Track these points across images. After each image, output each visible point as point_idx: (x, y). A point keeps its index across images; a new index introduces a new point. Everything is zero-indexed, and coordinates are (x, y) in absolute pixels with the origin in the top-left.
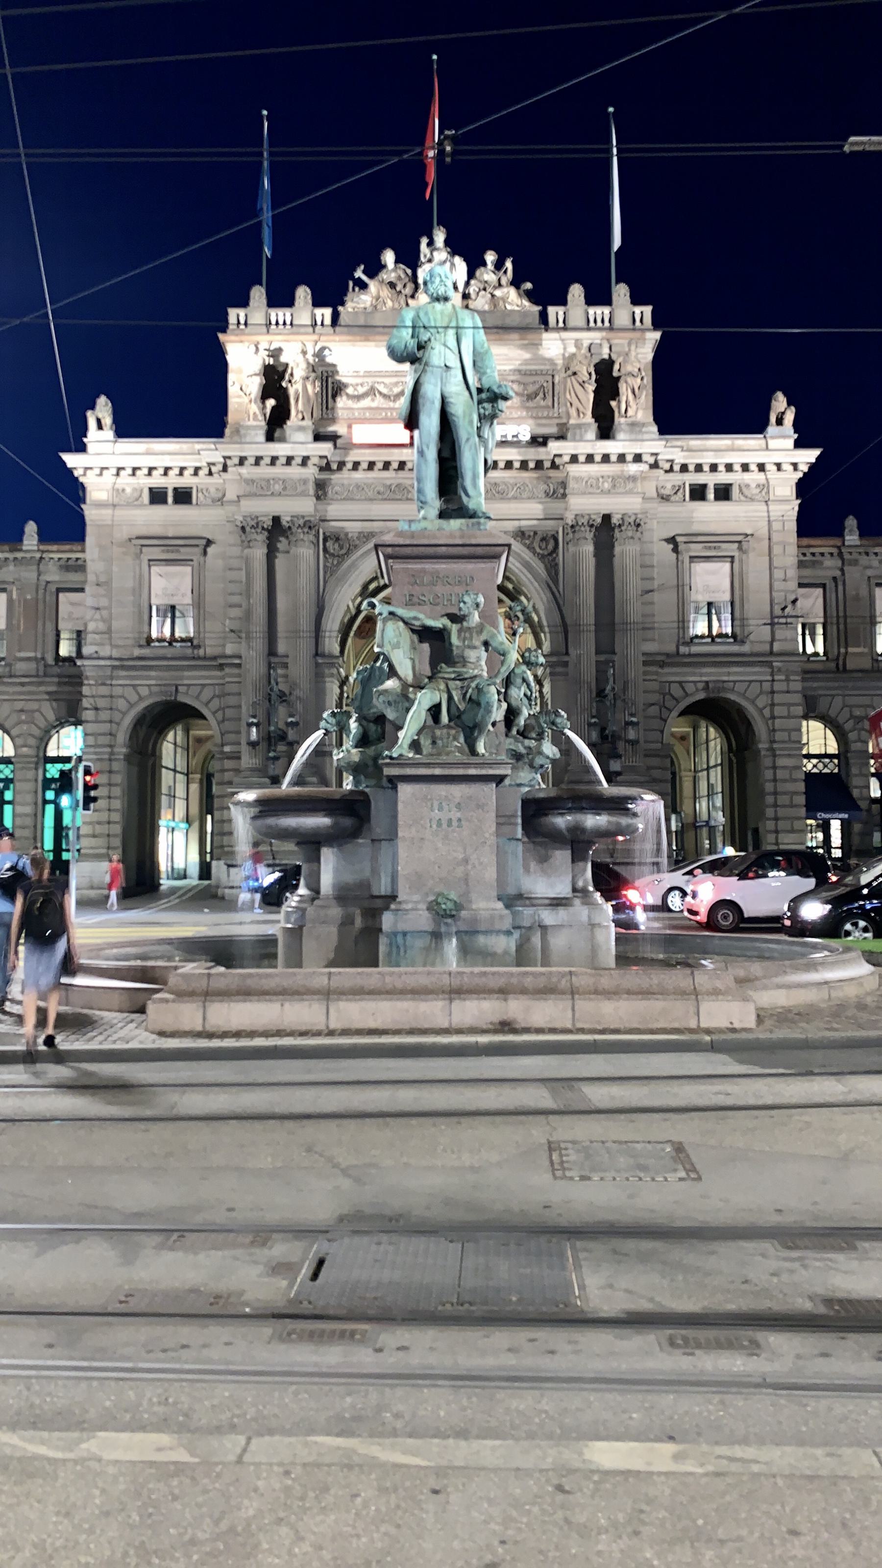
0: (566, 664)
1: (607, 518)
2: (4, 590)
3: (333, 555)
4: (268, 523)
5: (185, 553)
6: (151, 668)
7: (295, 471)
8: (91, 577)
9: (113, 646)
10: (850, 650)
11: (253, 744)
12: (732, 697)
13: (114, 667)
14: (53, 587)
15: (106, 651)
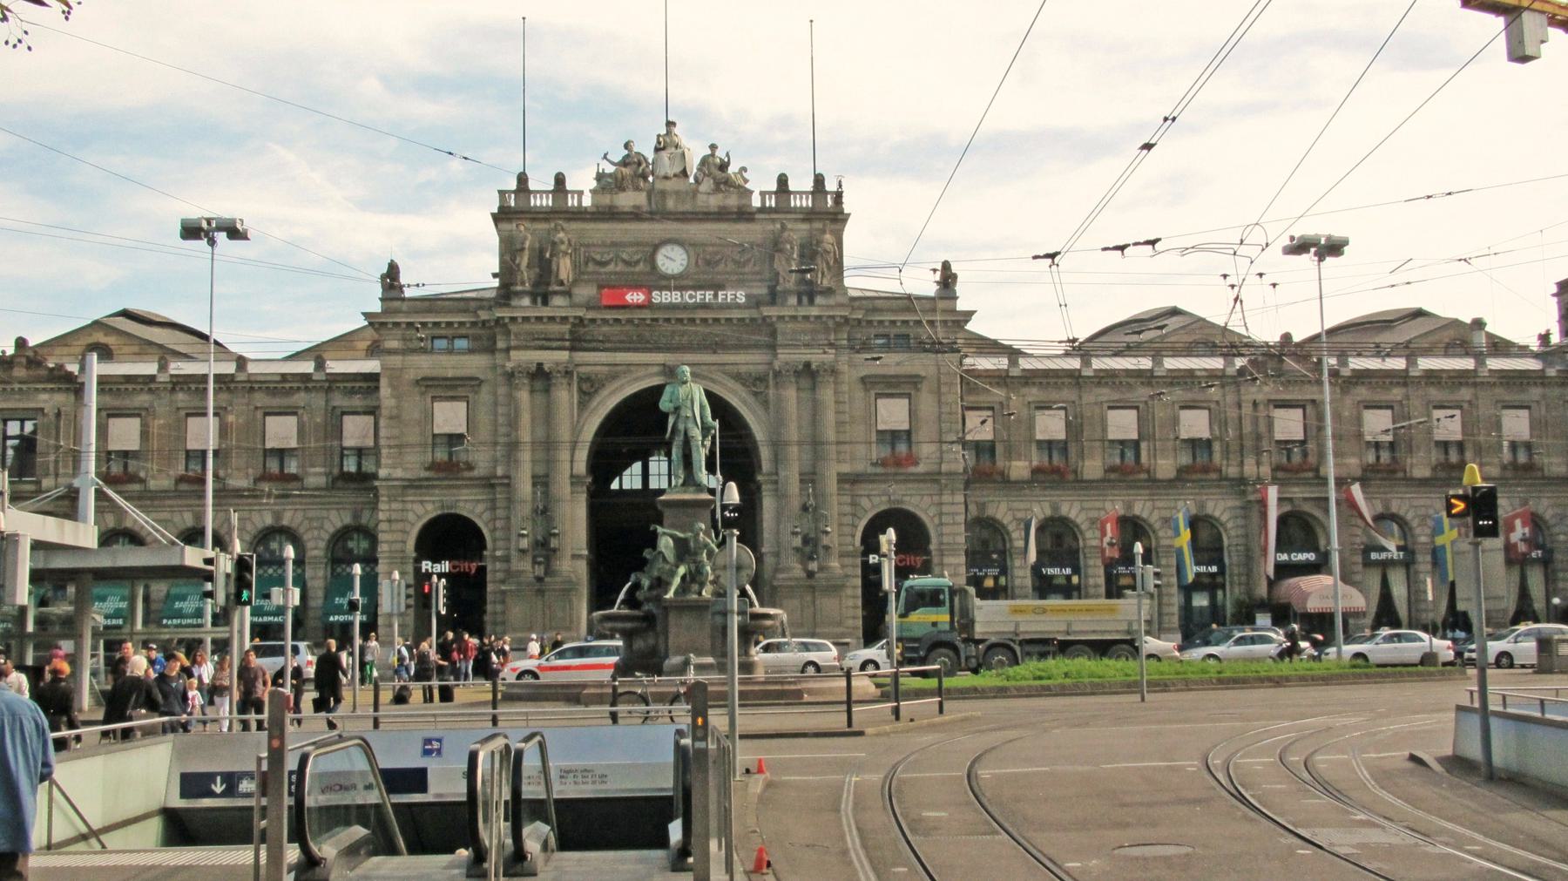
0: (776, 482)
1: (807, 365)
2: (295, 414)
3: (585, 393)
4: (533, 368)
5: (461, 392)
6: (434, 487)
7: (555, 328)
8: (384, 412)
9: (405, 469)
10: (1014, 463)
11: (523, 551)
12: (911, 509)
13: (405, 487)
14: (338, 412)
15: (399, 473)
